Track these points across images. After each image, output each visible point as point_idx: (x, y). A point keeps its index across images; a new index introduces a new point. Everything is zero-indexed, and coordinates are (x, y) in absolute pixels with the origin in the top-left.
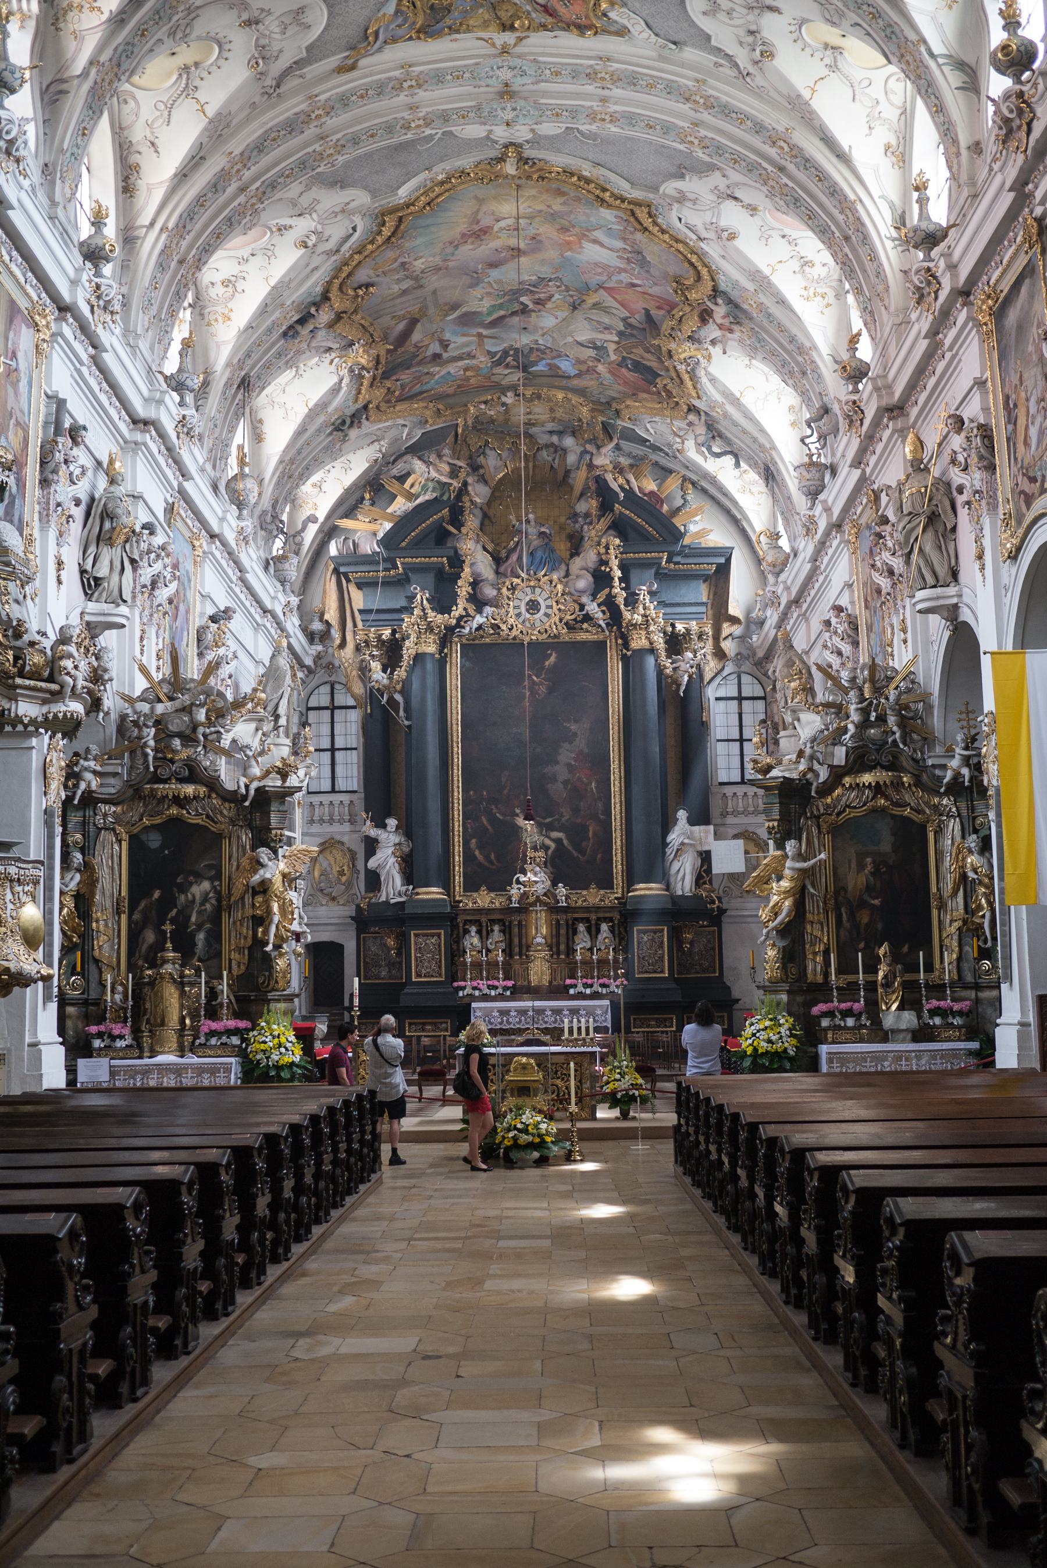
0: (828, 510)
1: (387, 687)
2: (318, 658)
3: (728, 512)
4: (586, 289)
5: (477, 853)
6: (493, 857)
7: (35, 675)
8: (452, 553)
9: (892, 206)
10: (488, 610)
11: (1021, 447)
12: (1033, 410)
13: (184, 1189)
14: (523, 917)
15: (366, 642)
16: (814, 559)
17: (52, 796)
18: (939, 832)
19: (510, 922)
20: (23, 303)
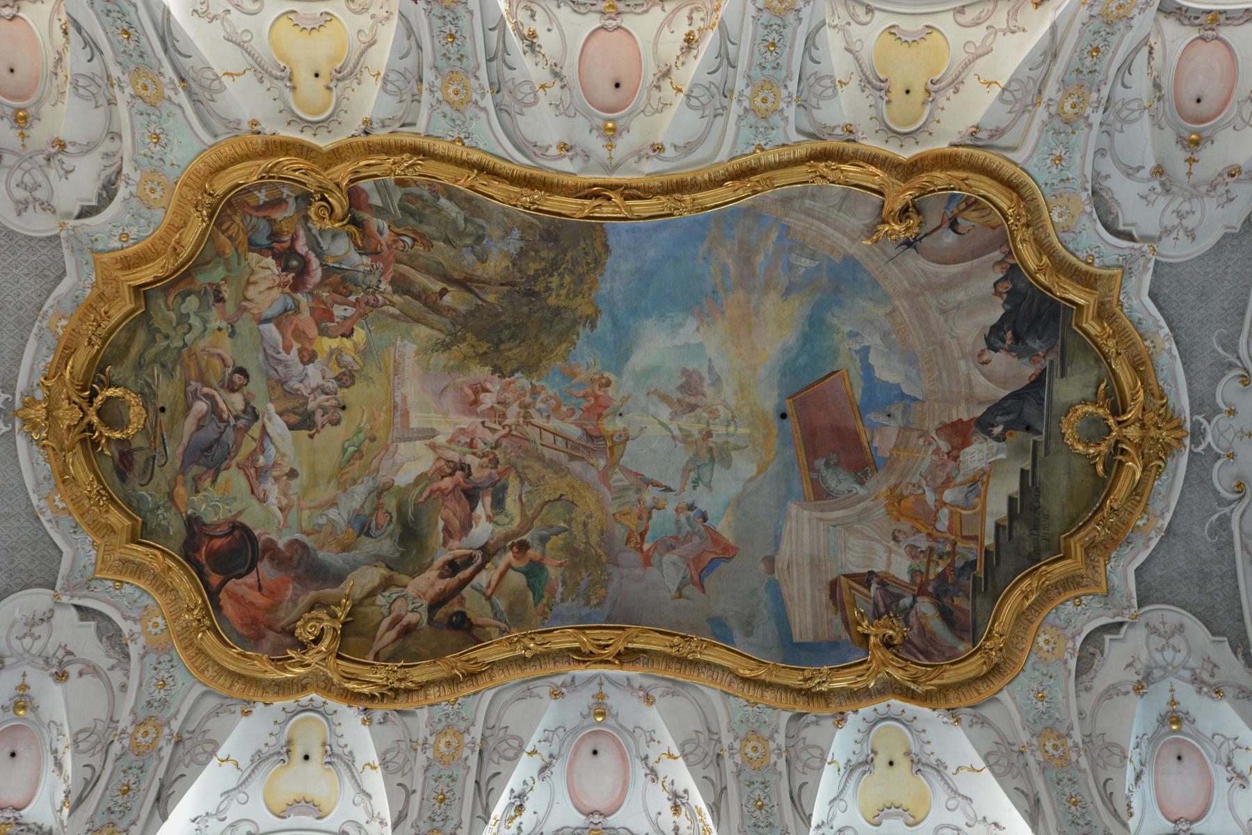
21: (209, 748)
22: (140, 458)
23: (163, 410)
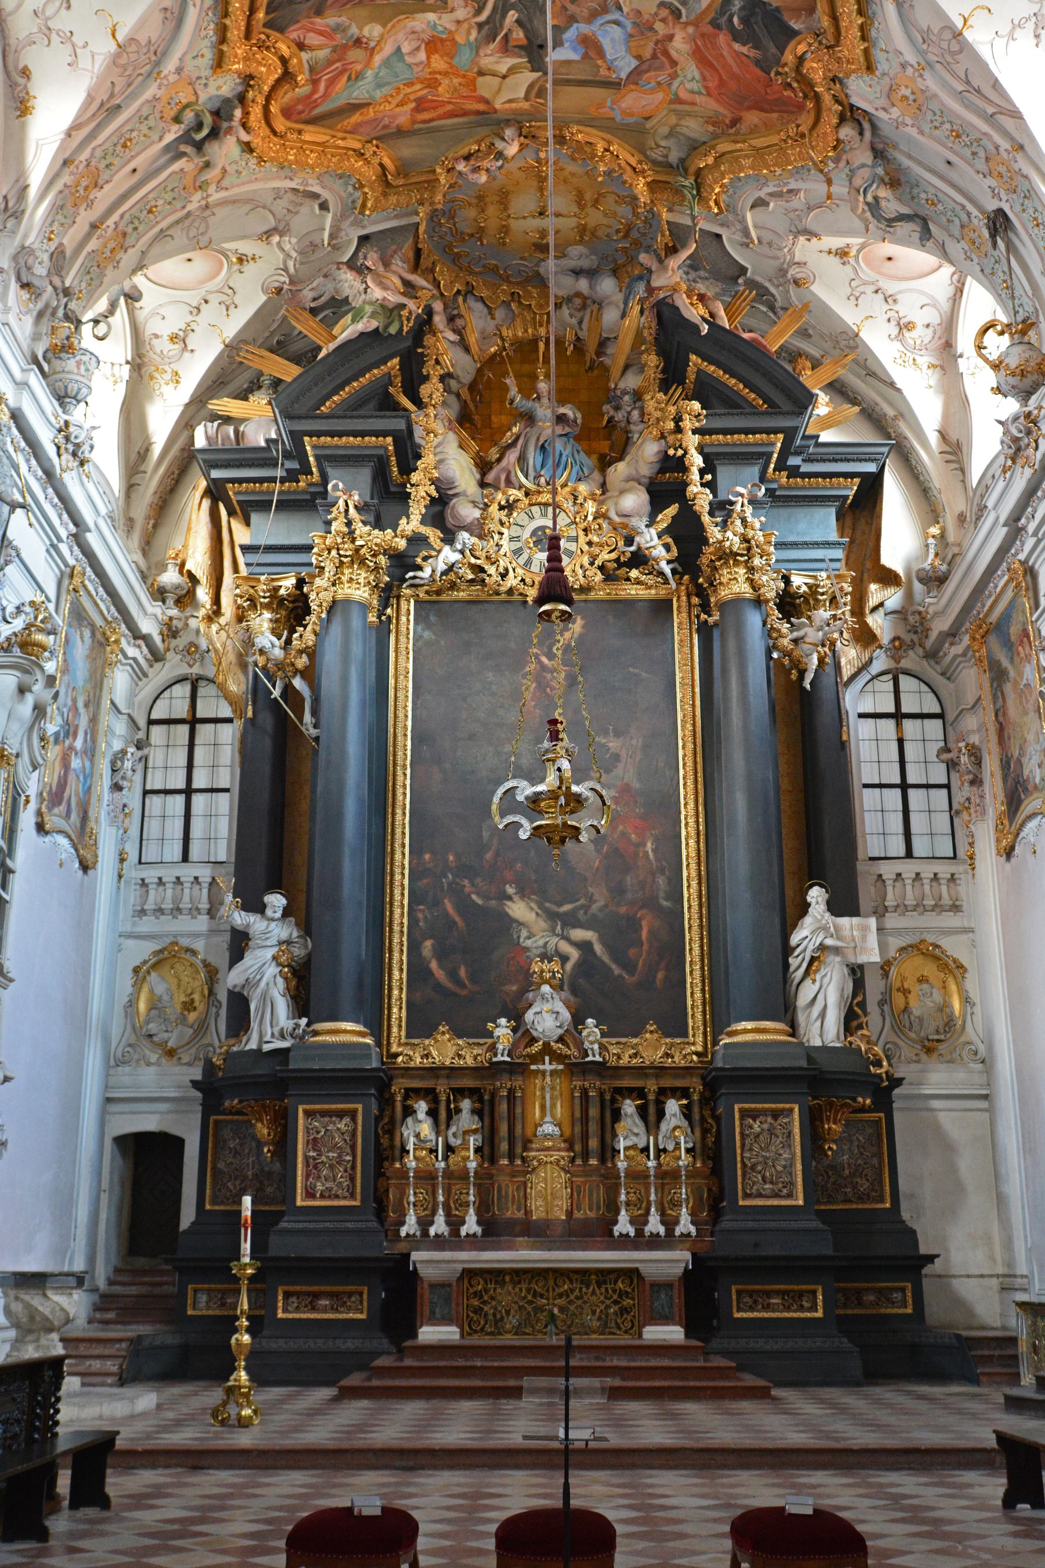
1: (280, 666)
2: (170, 631)
5: (434, 965)
6: (462, 973)
8: (401, 425)
10: (464, 536)
14: (518, 1082)
15: (252, 599)
19: (493, 1095)
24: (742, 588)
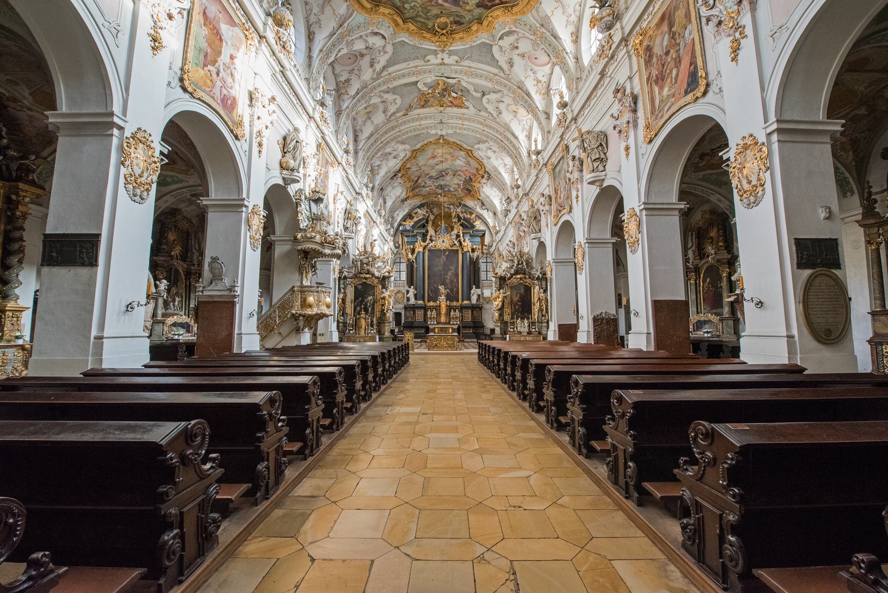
0: (509, 219)
2: (397, 252)
3: (485, 223)
4: (457, 171)
7: (329, 243)
9: (527, 149)
11: (558, 199)
12: (562, 190)
13: (356, 367)
16: (505, 231)
17: (336, 275)
18: (534, 288)
20: (330, 161)
21: (547, 18)
22: (457, 19)
23: (441, 12)
24: (467, 250)
